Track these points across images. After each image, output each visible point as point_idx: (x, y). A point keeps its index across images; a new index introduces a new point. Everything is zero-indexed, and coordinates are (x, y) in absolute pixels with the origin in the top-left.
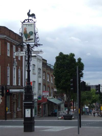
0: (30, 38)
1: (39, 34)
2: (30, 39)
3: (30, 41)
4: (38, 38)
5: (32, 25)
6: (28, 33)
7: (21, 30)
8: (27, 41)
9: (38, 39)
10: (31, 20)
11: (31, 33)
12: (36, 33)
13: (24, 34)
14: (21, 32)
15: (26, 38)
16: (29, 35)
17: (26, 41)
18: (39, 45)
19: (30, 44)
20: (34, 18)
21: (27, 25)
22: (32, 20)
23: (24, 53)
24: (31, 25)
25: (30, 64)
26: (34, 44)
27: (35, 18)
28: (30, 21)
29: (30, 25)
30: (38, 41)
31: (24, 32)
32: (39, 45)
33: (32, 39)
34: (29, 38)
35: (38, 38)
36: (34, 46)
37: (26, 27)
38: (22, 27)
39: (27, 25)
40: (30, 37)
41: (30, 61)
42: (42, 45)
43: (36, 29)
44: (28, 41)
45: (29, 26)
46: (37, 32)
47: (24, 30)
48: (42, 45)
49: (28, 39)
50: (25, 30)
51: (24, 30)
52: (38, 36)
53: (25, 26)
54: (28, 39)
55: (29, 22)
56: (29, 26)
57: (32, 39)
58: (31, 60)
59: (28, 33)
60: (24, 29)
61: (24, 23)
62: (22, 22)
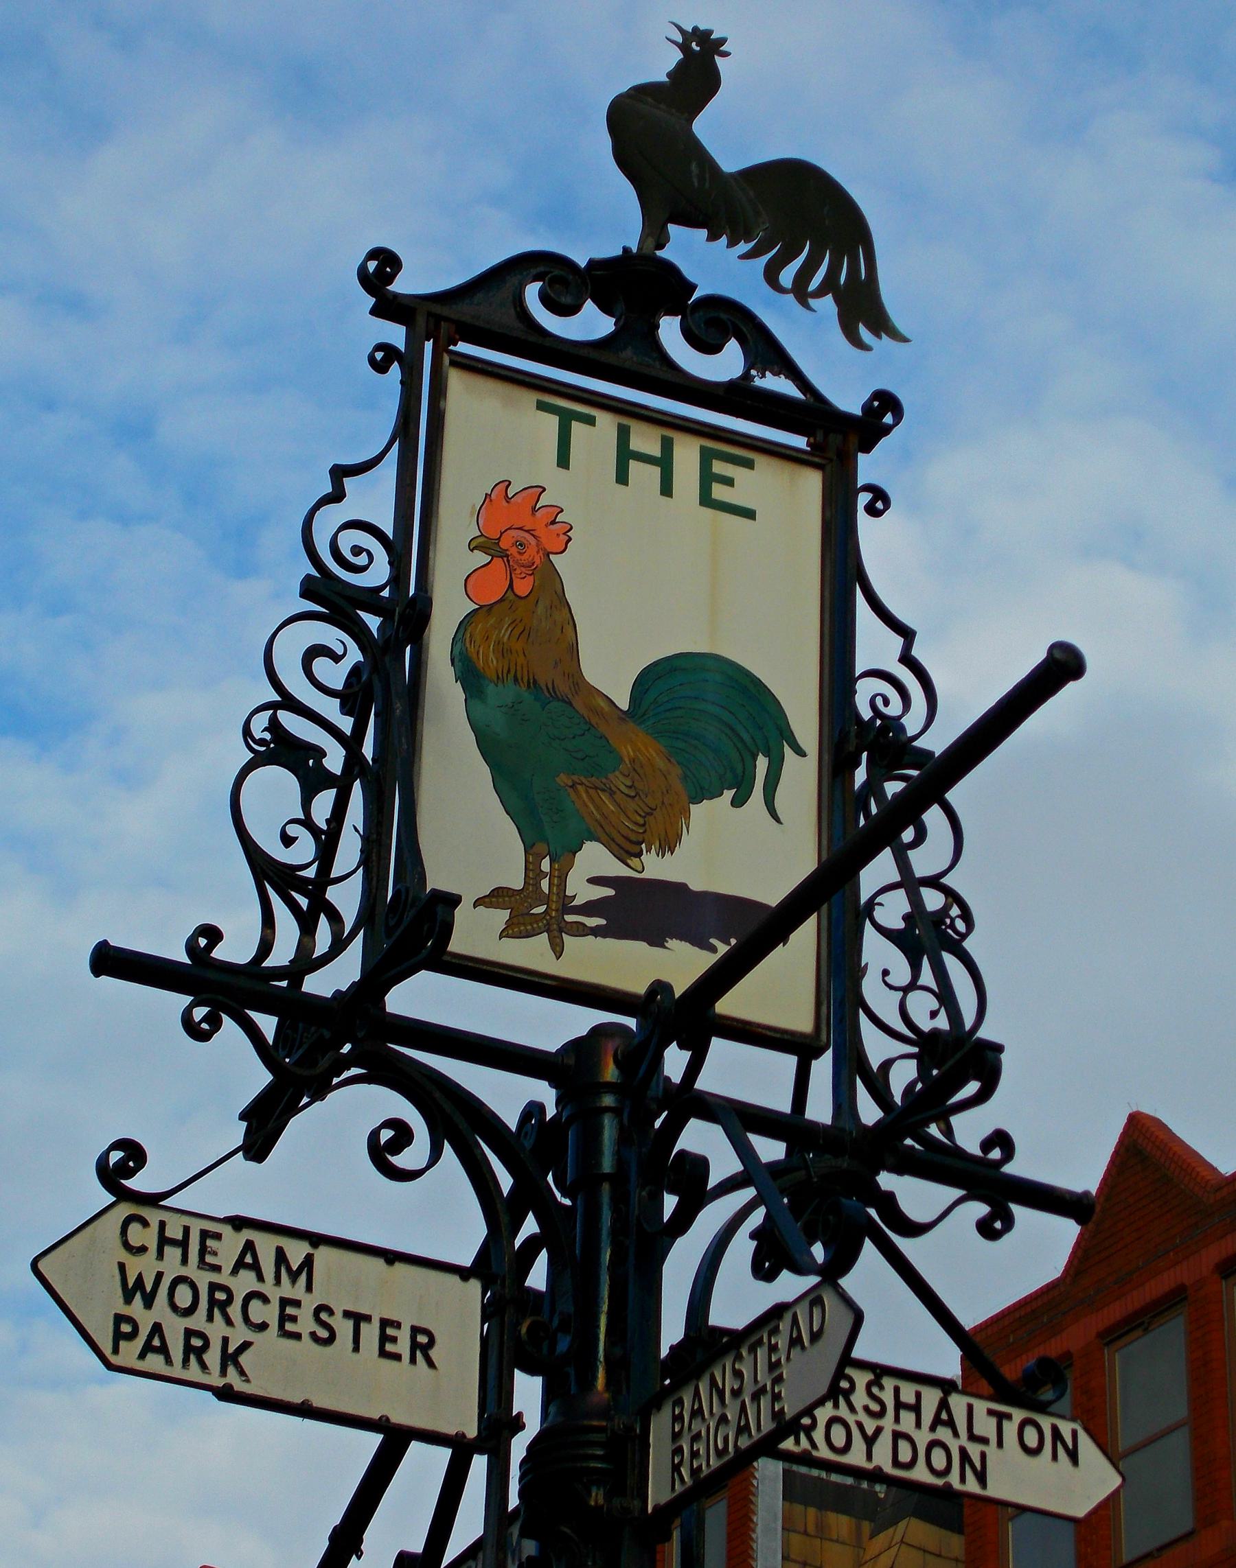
0: (655, 866)
6: (610, 671)
10: (717, 321)
20: (827, 305)
22: (766, 351)
23: (423, 1345)
24: (707, 479)
27: (863, 311)
29: (687, 453)
34: (627, 851)
40: (668, 844)
45: (644, 476)
49: (595, 860)
50: (524, 542)
54: (595, 860)
56: (644, 476)
59: (610, 671)
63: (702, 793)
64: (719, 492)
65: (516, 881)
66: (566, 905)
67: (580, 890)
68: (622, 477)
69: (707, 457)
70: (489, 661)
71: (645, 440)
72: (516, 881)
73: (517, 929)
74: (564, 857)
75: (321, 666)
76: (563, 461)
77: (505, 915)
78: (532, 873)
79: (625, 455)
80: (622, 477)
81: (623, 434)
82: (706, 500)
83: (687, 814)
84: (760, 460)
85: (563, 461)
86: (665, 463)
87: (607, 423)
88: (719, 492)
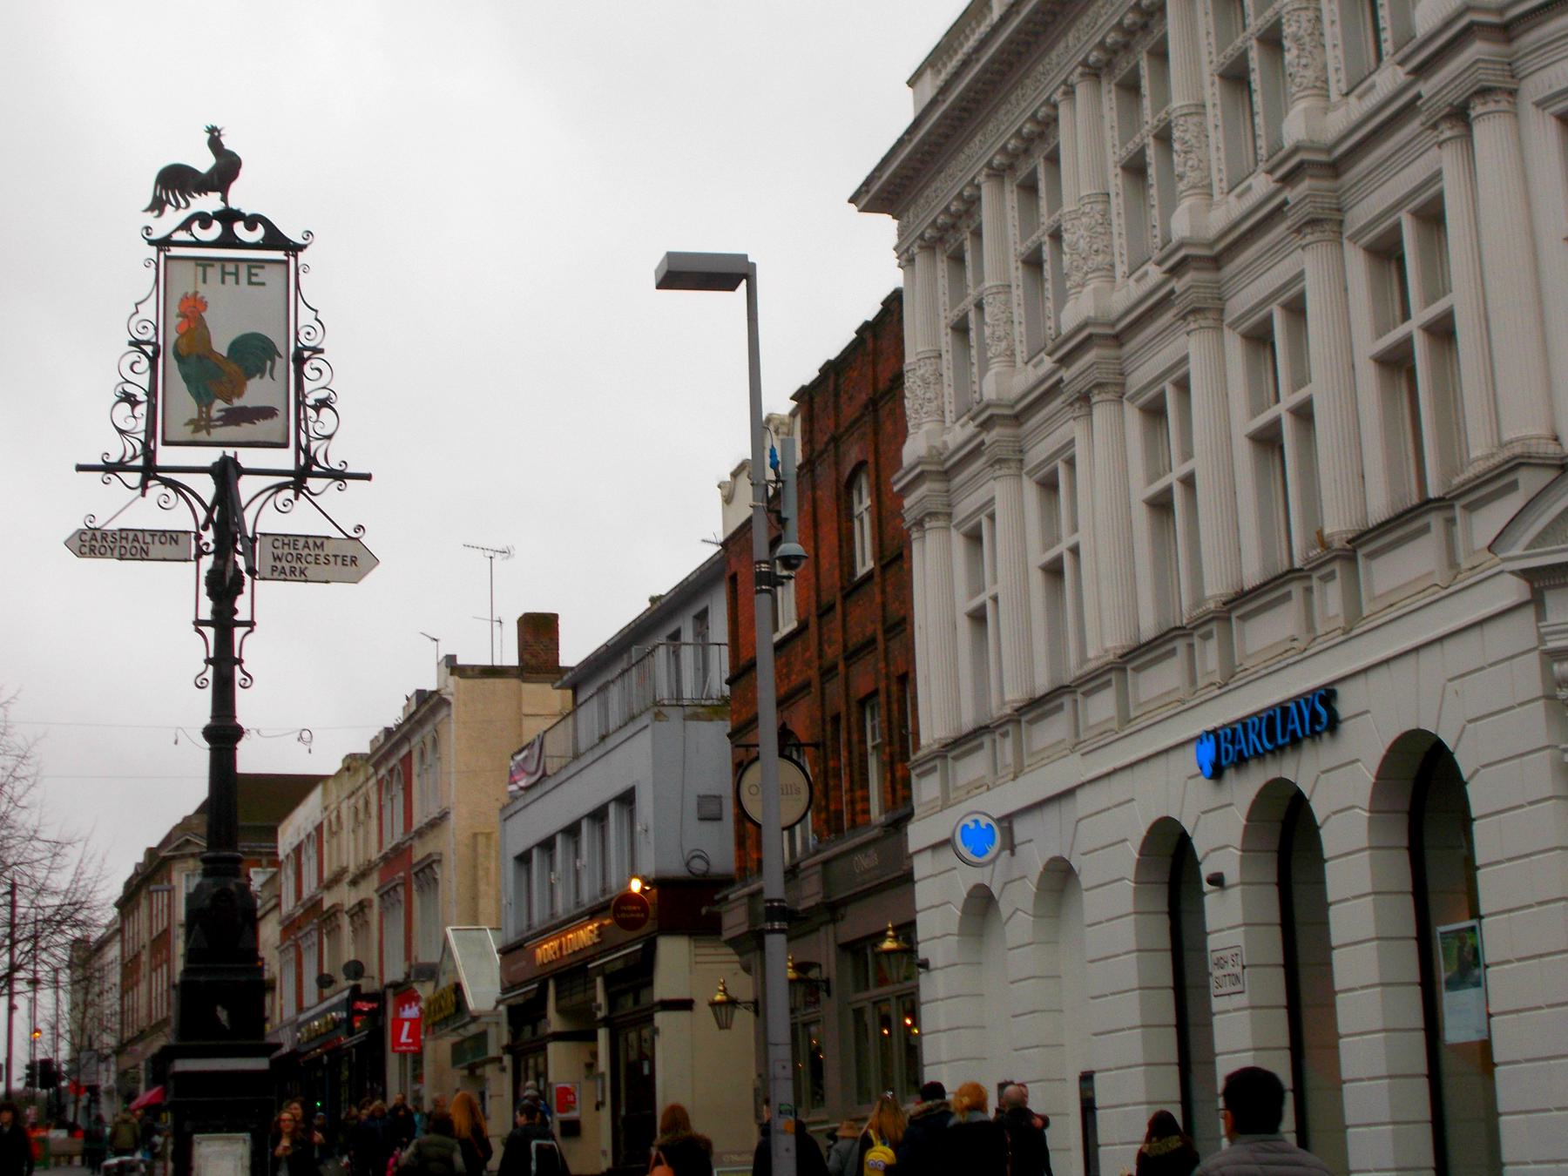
0: (237, 403)
1: (343, 369)
2: (243, 409)
3: (246, 426)
4: (323, 404)
5: (262, 275)
6: (221, 345)
7: (148, 311)
8: (208, 428)
9: (325, 411)
11: (255, 353)
12: (306, 354)
13: (178, 356)
14: (149, 335)
15: (203, 399)
16: (233, 367)
17: (202, 423)
18: (339, 476)
19: (247, 458)
21: (214, 273)
24: (250, 275)
25: (240, 661)
26: (285, 459)
28: (239, 229)
30: (329, 437)
31: (173, 336)
32: (339, 476)
33: (267, 413)
34: (228, 401)
35: (323, 404)
36: (280, 487)
37: (203, 291)
38: (163, 282)
39: (214, 273)
40: (240, 395)
41: (239, 632)
42: (368, 477)
43: (306, 317)
44: (219, 433)
45: (230, 279)
46: (317, 351)
47: (175, 321)
48: (368, 477)
49: (219, 405)
50: (192, 312)
51: (182, 315)
52: (322, 383)
53: (186, 282)
54: (219, 405)
55: (228, 240)
56: (230, 279)
57: (267, 413)
58: (251, 624)
59: (221, 345)
60: (174, 309)
61: (175, 251)
62: (156, 235)
63: (250, 376)
64: (254, 279)
65: (196, 416)
66: (210, 419)
67: (215, 414)
68: (223, 282)
69: (249, 268)
70: (184, 350)
71: (230, 268)
72: (196, 416)
73: (196, 430)
74: (209, 406)
75: (137, 368)
76: (205, 281)
77: (191, 428)
78: (200, 412)
79: (224, 273)
80: (223, 282)
81: (223, 268)
82: (250, 283)
83: (244, 384)
84: (267, 266)
85: (205, 281)
86: (236, 274)
87: (218, 265)
88: (254, 279)
